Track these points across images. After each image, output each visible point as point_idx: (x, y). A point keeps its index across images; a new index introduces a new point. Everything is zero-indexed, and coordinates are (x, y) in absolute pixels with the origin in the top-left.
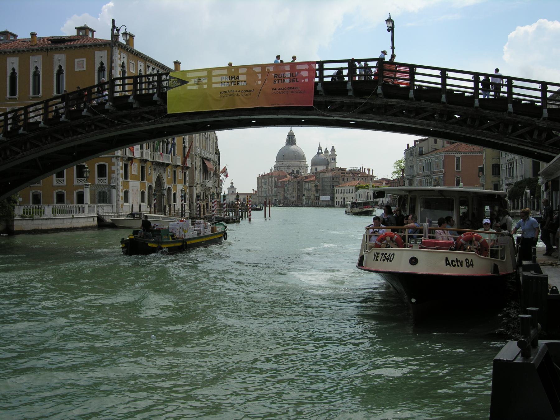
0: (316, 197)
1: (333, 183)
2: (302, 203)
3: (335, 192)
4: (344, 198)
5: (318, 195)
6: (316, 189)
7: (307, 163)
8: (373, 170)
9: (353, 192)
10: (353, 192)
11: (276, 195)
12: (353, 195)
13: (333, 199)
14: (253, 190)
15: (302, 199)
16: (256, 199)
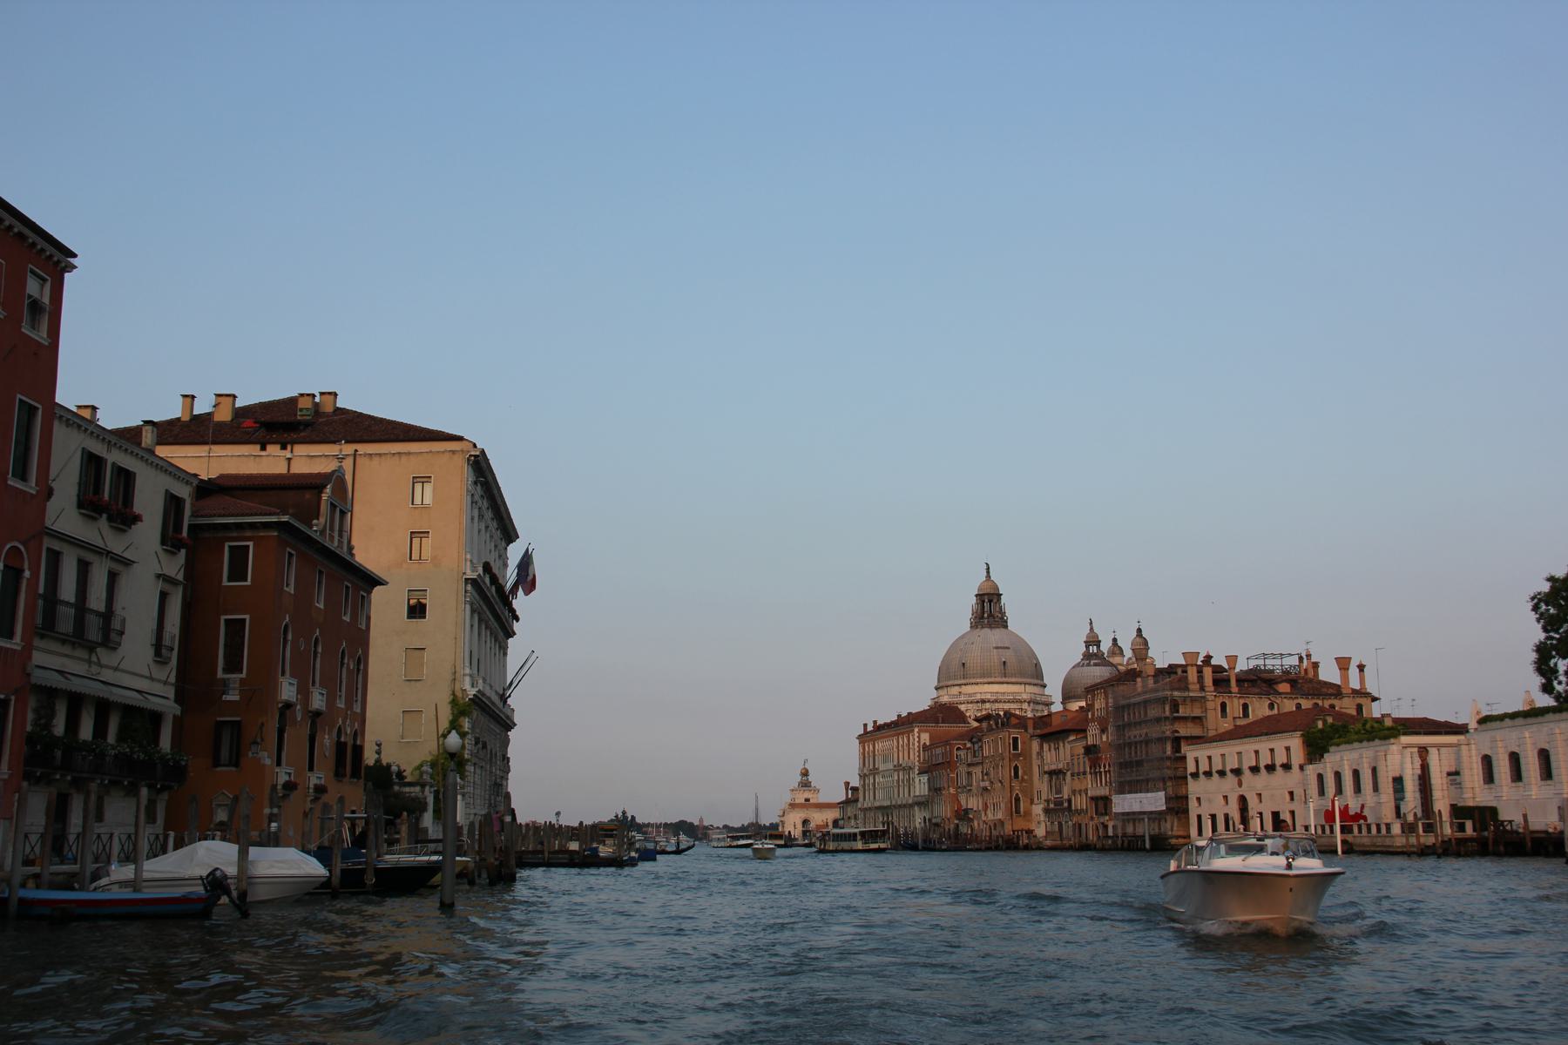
0: (1095, 799)
1: (1177, 726)
2: (1029, 832)
3: (1191, 768)
4: (1243, 800)
5: (1103, 791)
6: (1095, 764)
7: (1047, 691)
8: (1361, 668)
9: (1295, 767)
10: (1296, 762)
11: (922, 803)
12: (1293, 779)
13: (1178, 806)
14: (847, 784)
15: (1028, 814)
16: (856, 817)
